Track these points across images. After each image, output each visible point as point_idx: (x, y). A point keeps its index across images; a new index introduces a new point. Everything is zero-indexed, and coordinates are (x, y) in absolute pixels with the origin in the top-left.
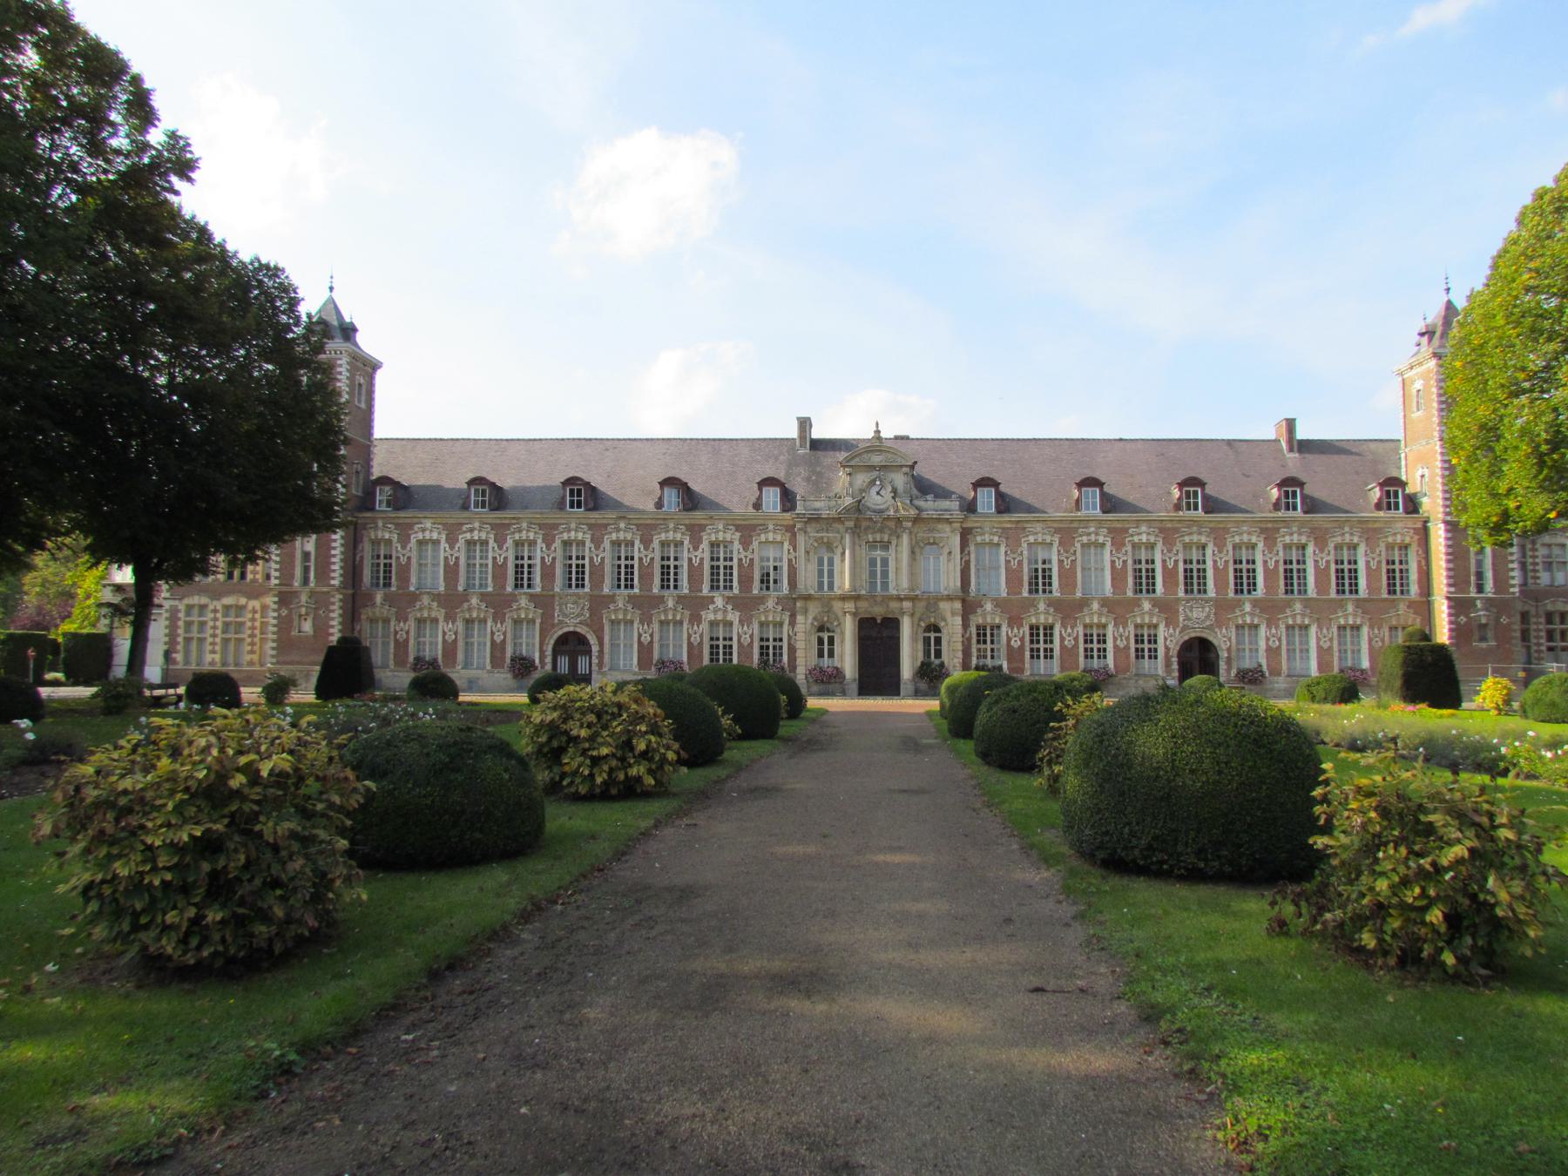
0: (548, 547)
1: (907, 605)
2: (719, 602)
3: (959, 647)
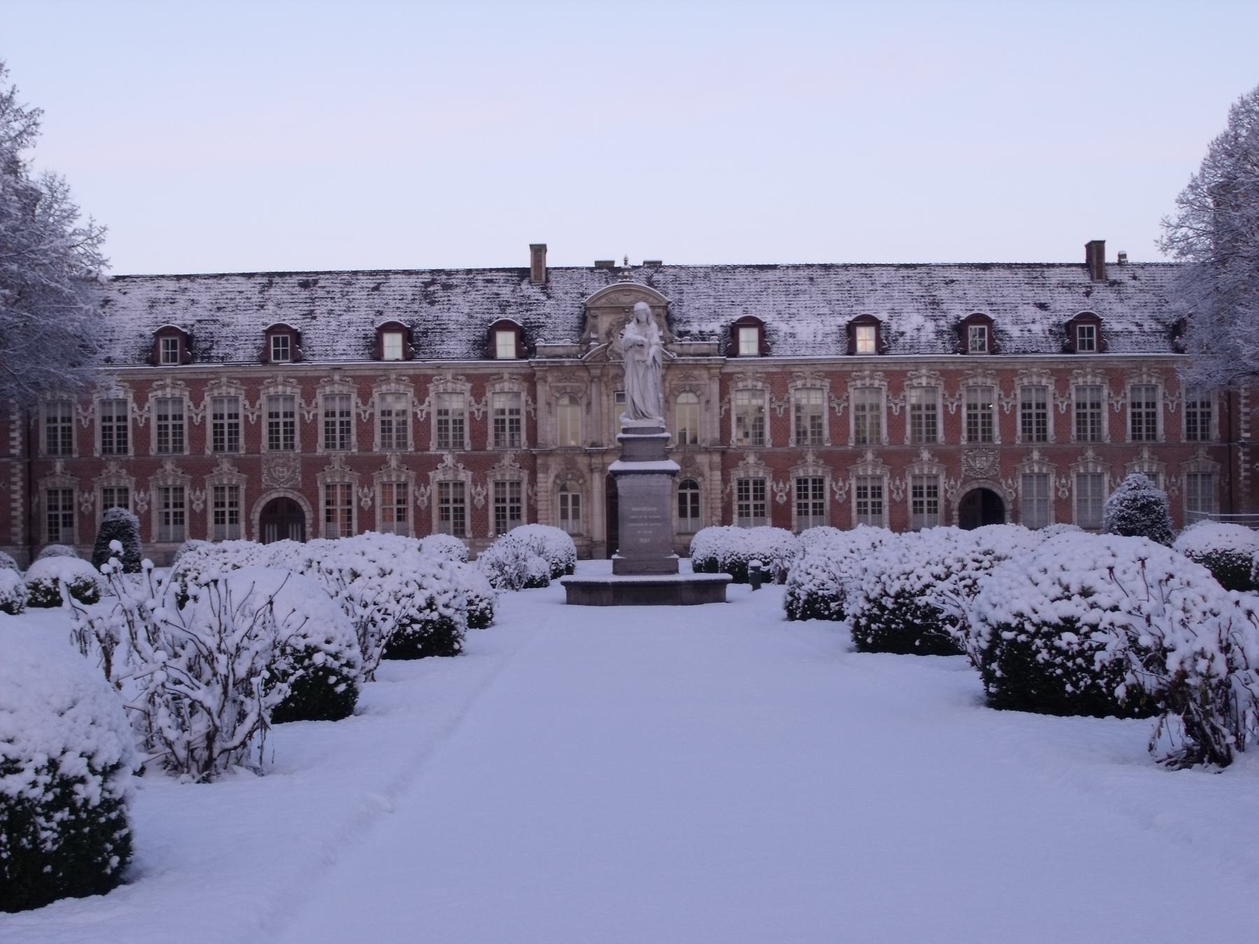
0: (252, 404)
2: (449, 459)
3: (719, 504)
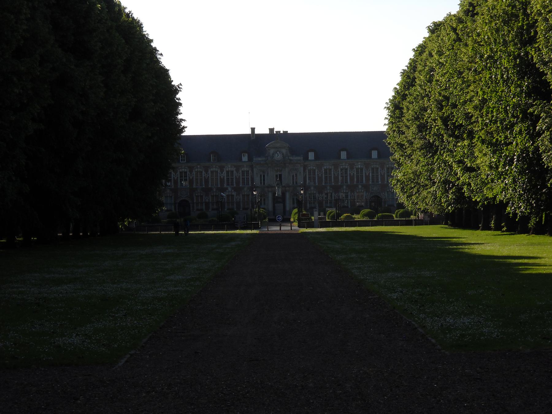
0: (176, 174)
1: (287, 188)
2: (230, 189)
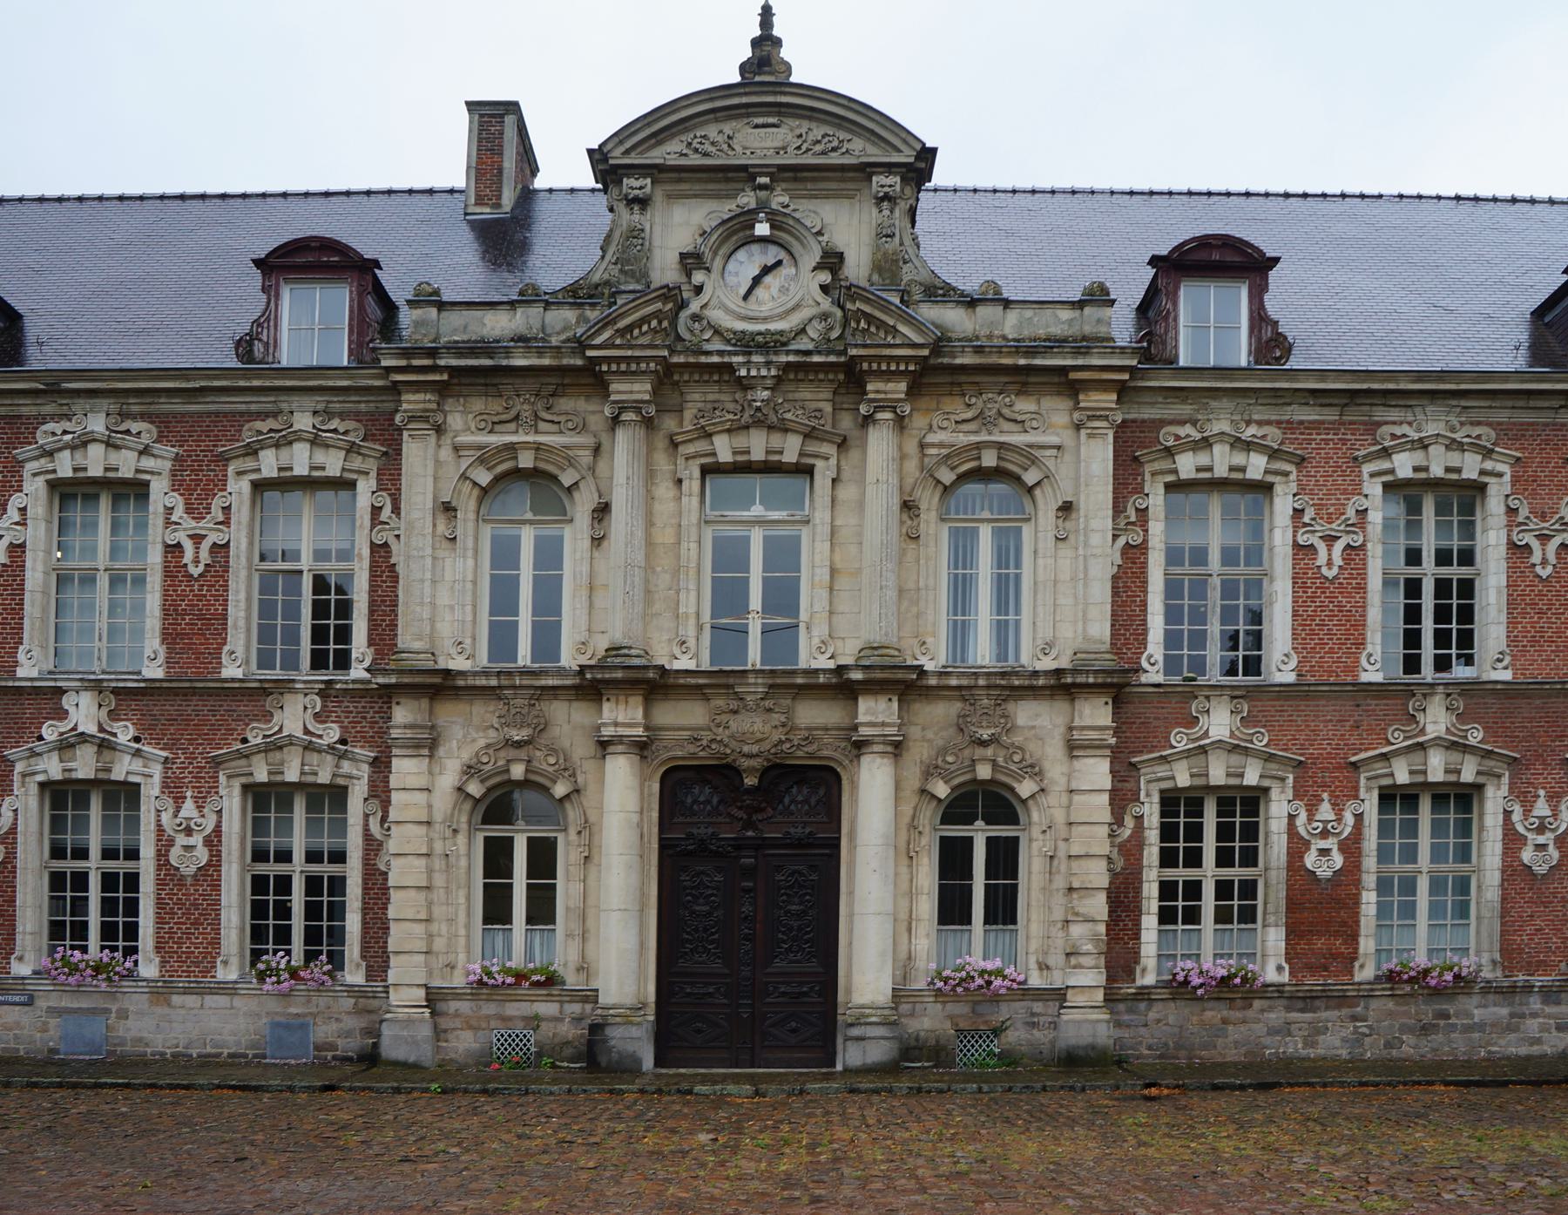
1: (875, 712)
3: (1098, 875)
